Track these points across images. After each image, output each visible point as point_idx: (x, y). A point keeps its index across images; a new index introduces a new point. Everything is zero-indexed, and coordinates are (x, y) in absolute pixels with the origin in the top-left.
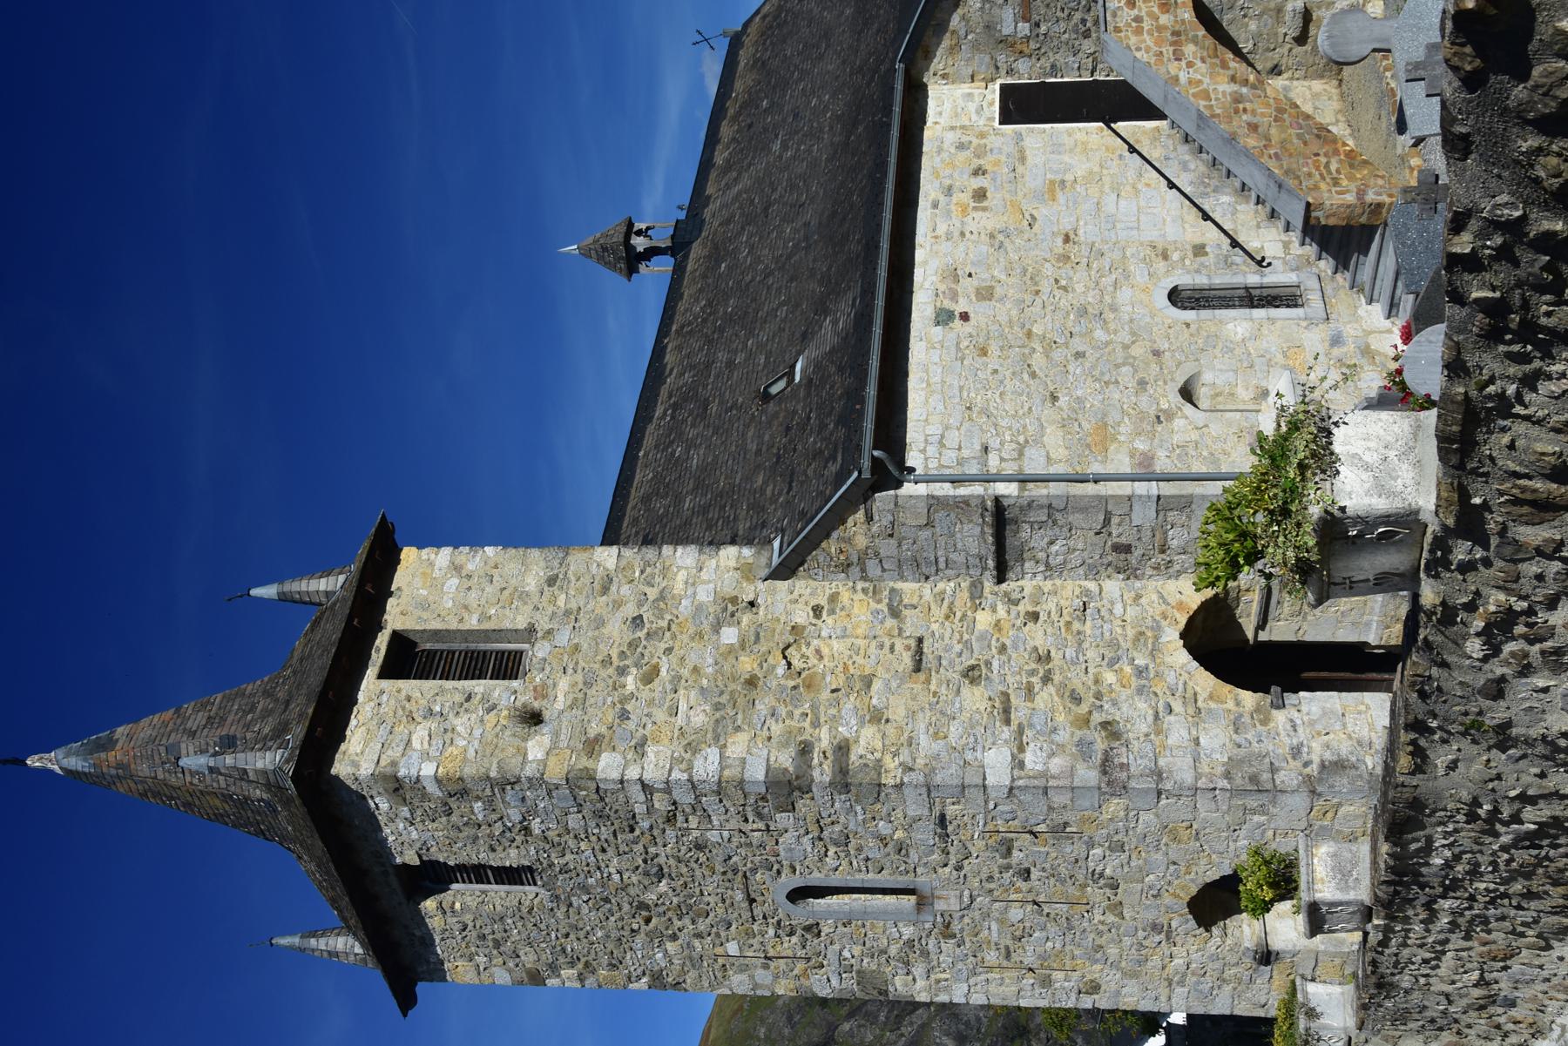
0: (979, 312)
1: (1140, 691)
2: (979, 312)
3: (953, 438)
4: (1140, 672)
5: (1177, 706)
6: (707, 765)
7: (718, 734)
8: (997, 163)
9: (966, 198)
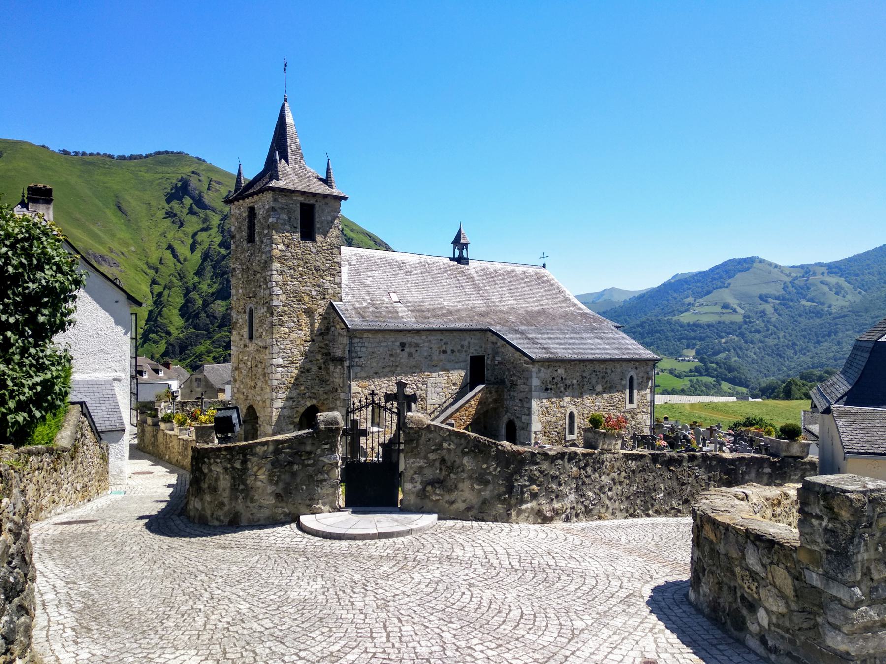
0: (405, 354)
1: (299, 394)
2: (405, 354)
3: (363, 349)
4: (304, 394)
5: (294, 404)
6: (277, 290)
7: (285, 292)
8: (456, 356)
9: (444, 348)
